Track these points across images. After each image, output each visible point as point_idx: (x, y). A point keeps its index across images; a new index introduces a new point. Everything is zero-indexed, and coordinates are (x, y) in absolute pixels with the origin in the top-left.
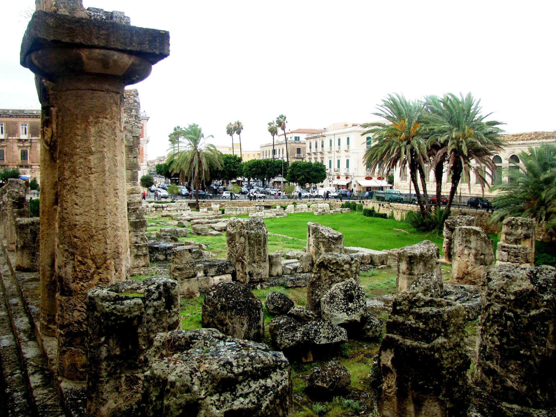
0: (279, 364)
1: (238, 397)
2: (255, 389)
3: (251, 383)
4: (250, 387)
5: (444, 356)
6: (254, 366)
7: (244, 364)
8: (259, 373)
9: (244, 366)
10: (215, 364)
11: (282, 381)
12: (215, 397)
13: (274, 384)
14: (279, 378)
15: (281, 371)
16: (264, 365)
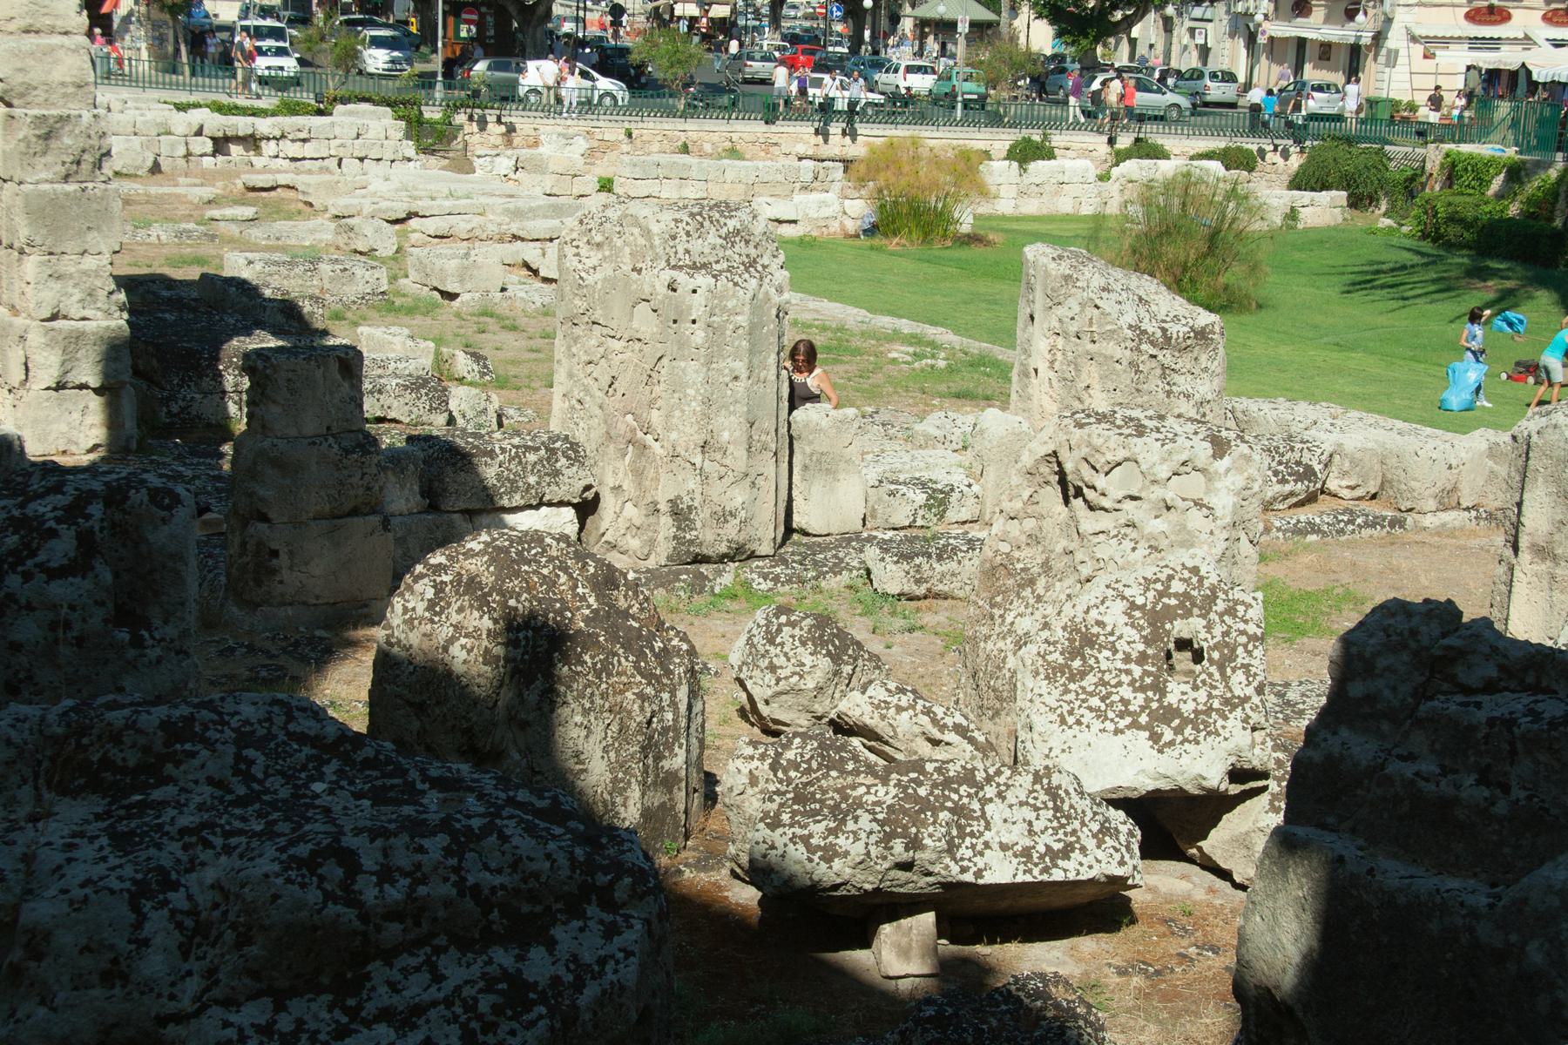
0: (602, 879)
1: (368, 1024)
2: (458, 989)
4: (438, 978)
6: (471, 880)
8: (495, 914)
9: (417, 876)
10: (270, 851)
11: (602, 961)
13: (561, 970)
14: (590, 947)
15: (608, 918)
16: (525, 880)
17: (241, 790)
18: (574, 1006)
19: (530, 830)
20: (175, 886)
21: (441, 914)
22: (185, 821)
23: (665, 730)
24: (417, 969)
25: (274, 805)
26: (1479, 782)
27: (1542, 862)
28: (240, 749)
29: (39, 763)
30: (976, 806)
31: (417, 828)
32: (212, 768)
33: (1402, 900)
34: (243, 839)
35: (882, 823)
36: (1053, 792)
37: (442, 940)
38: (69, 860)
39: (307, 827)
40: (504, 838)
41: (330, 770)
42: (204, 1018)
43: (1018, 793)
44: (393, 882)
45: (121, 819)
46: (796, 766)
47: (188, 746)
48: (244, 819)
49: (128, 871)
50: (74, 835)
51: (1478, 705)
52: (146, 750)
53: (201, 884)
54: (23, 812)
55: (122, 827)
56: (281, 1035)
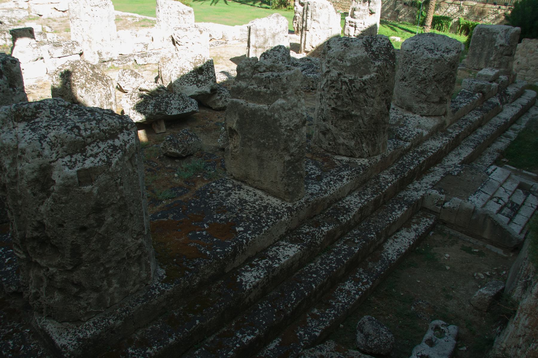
0: (125, 125)
1: (88, 157)
2: (104, 149)
3: (100, 144)
4: (99, 147)
5: (283, 116)
6: (102, 129)
7: (91, 127)
8: (107, 134)
9: (92, 130)
10: (63, 129)
11: (129, 140)
12: (67, 159)
14: (126, 138)
15: (128, 132)
16: (111, 127)
17: (53, 117)
18: (125, 149)
19: (110, 118)
20: (46, 137)
21: (97, 135)
22: (44, 125)
23: (109, 94)
24: (95, 146)
25: (60, 119)
26: (264, 88)
27: (276, 100)
28: (50, 109)
29: (12, 117)
30: (169, 101)
31: (89, 120)
32: (46, 114)
33: (253, 109)
34: (56, 127)
35: (153, 107)
36: (182, 97)
37: (98, 140)
38: (25, 135)
39: (68, 123)
40: (106, 120)
41: (68, 111)
42: (58, 161)
43: (176, 99)
44: (87, 131)
45: (31, 126)
46: (135, 98)
47: (40, 110)
48: (55, 123)
49: (37, 136)
50: (24, 130)
51: (263, 75)
52: (32, 112)
53: (51, 136)
54: (12, 126)
55: (32, 127)
56: (73, 162)
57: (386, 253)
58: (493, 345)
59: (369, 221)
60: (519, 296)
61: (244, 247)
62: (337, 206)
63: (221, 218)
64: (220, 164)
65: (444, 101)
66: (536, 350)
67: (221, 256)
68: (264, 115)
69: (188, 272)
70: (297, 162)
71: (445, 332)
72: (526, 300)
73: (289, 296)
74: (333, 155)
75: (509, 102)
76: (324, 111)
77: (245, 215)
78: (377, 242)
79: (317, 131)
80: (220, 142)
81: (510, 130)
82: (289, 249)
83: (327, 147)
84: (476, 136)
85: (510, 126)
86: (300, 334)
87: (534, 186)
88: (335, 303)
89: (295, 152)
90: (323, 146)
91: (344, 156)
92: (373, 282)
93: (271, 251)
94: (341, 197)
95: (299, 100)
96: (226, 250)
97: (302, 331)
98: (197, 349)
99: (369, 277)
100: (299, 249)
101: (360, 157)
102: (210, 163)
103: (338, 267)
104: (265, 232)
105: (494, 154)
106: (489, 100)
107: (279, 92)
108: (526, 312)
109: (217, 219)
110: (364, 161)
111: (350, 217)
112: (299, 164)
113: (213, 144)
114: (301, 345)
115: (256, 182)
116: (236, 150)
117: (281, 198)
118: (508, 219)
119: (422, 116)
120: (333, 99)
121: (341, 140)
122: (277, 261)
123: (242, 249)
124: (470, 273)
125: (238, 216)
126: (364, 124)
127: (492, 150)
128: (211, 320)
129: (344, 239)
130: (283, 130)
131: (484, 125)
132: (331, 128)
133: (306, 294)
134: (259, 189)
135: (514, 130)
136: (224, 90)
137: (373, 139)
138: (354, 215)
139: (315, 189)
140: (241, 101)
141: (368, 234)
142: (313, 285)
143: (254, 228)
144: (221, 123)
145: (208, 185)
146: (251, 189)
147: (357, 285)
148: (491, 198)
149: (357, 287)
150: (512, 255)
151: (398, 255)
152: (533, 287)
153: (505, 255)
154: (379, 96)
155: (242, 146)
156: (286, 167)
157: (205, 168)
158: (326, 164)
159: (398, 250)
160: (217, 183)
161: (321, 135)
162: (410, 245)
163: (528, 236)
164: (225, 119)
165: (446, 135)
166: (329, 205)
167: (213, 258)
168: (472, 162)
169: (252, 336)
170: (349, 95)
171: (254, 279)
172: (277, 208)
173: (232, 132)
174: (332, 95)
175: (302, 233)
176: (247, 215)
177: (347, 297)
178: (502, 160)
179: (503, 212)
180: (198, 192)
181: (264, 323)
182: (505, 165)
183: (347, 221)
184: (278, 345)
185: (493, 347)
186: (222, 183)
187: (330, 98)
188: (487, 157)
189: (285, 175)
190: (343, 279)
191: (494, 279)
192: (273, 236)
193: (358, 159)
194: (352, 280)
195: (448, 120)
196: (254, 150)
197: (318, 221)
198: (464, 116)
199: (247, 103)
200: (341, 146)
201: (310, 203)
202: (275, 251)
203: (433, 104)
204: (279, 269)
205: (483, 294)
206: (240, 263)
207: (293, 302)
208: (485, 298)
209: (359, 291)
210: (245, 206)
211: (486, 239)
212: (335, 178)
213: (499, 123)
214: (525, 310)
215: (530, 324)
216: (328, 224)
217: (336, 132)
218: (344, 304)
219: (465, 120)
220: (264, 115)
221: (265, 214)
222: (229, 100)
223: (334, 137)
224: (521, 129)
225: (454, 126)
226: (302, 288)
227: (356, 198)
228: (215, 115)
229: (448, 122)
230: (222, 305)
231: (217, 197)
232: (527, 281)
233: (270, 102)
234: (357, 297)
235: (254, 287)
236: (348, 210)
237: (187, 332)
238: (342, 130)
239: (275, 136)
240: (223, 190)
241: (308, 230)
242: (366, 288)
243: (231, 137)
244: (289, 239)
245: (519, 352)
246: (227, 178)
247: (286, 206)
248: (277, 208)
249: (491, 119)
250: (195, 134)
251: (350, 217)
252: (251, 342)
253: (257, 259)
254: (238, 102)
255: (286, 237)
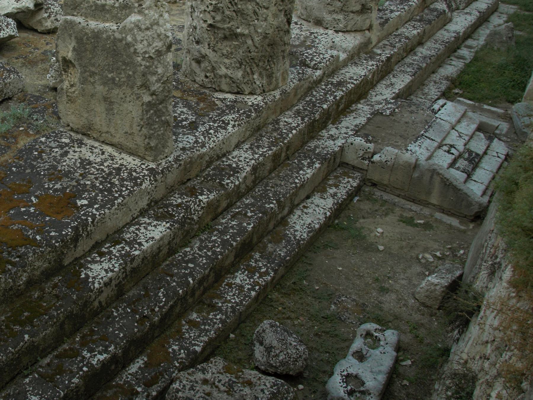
5: (139, 38)
27: (128, 16)
33: (96, 31)
57: (292, 230)
58: (449, 357)
59: (267, 185)
60: (485, 285)
61: (89, 228)
62: (219, 164)
63: (56, 187)
64: (51, 110)
65: (368, 9)
66: (511, 362)
67: (57, 242)
68: (112, 37)
69: (10, 267)
70: (161, 103)
71: (379, 340)
72: (495, 290)
73: (156, 295)
74: (213, 92)
75: (461, 8)
76: (198, 30)
77: (89, 183)
78: (278, 214)
79: (188, 59)
80: (50, 79)
81: (462, 48)
82: (153, 228)
83: (202, 80)
84: (415, 58)
85: (463, 42)
86: (173, 349)
87: (500, 127)
88: (222, 303)
89: (158, 89)
90: (198, 79)
91: (227, 93)
92: (275, 271)
93: (128, 232)
94: (225, 151)
95: (161, 15)
96: (64, 233)
97: (176, 345)
98: (27, 376)
99: (269, 265)
100: (168, 228)
101: (251, 94)
102: (37, 110)
103: (225, 251)
104: (118, 206)
105: (441, 83)
106: (432, 7)
107: (133, 4)
108: (494, 307)
109: (49, 188)
110: (257, 99)
111: (239, 180)
112: (164, 107)
113: (40, 82)
114: (175, 366)
115: (103, 135)
116: (73, 89)
117: (139, 156)
118: (465, 176)
119: (337, 32)
120: (209, 12)
121: (223, 71)
122: (137, 246)
123: (86, 230)
124: (413, 255)
125: (79, 184)
126: (255, 46)
127: (438, 77)
128: (46, 334)
129: (232, 212)
130: (139, 59)
131: (426, 41)
132: (208, 54)
133: (181, 291)
134: (107, 144)
135: (470, 47)
136: (53, 5)
137: (268, 67)
138: (245, 177)
139: (187, 142)
140: (78, 19)
141: (266, 203)
142: (190, 280)
143: (102, 200)
144: (50, 51)
145: (36, 141)
146: (96, 144)
147: (252, 277)
148: (440, 146)
149: (252, 280)
150: (471, 226)
151: (309, 232)
152: (503, 271)
153: (463, 228)
154: (275, 5)
155: (82, 84)
156: (146, 111)
157: (30, 116)
158: (202, 105)
159: (310, 224)
160: (48, 138)
161: (194, 64)
162: (326, 217)
163: (494, 199)
164: (57, 46)
165: (372, 58)
166: (209, 163)
167: (46, 245)
168: (410, 95)
169: (105, 355)
170: (232, 5)
171: (104, 273)
172: (135, 171)
173: (67, 63)
174: (208, 7)
175: (171, 205)
176: (92, 182)
177: (239, 294)
178: (454, 91)
179: (457, 165)
180: (21, 151)
181: (122, 335)
182: (458, 99)
183: (235, 185)
184: (143, 366)
185: (449, 358)
186: (55, 137)
187: (205, 11)
188: (431, 88)
189: (144, 123)
190: (232, 269)
191: (447, 261)
192: (130, 210)
193: (248, 97)
194: (245, 270)
195: (374, 36)
196: (100, 88)
197: (194, 188)
198: (397, 29)
199: (87, 21)
200: (223, 79)
201: (181, 162)
202: (134, 233)
203: (352, 14)
204: (141, 257)
205: (432, 284)
206: (84, 251)
207: (161, 304)
208: (435, 290)
209: (256, 286)
210: (88, 168)
211: (434, 205)
212: (216, 125)
213: (448, 39)
214: (494, 304)
215: (500, 324)
216: (209, 190)
217: (216, 60)
218: (235, 305)
219: (398, 35)
220: (112, 37)
221: (118, 180)
222: (62, 18)
223: (213, 67)
224: (480, 47)
225: (384, 45)
226: (174, 284)
227: (246, 152)
228: (42, 41)
229: (374, 40)
230: (61, 312)
231: (49, 158)
232: (495, 263)
233: (120, 19)
234: (253, 293)
235: (106, 284)
236: (236, 170)
237: (12, 352)
238: (223, 55)
239: (128, 68)
240: (56, 148)
241: (179, 201)
242: (265, 281)
243: (65, 72)
244: (153, 214)
245: (486, 365)
246: (61, 129)
247: (147, 167)
248: (135, 171)
249: (436, 33)
250: (14, 69)
251: (239, 180)
252: (104, 364)
253: (109, 245)
254: (74, 21)
255: (149, 212)
